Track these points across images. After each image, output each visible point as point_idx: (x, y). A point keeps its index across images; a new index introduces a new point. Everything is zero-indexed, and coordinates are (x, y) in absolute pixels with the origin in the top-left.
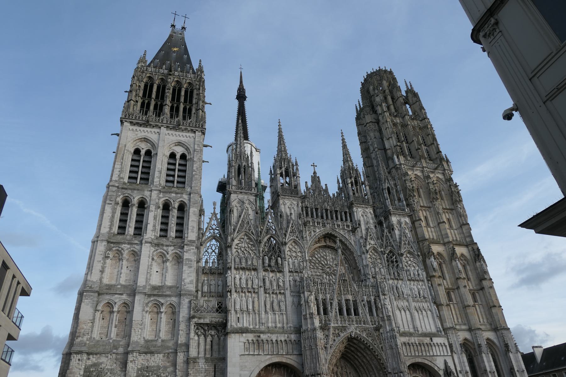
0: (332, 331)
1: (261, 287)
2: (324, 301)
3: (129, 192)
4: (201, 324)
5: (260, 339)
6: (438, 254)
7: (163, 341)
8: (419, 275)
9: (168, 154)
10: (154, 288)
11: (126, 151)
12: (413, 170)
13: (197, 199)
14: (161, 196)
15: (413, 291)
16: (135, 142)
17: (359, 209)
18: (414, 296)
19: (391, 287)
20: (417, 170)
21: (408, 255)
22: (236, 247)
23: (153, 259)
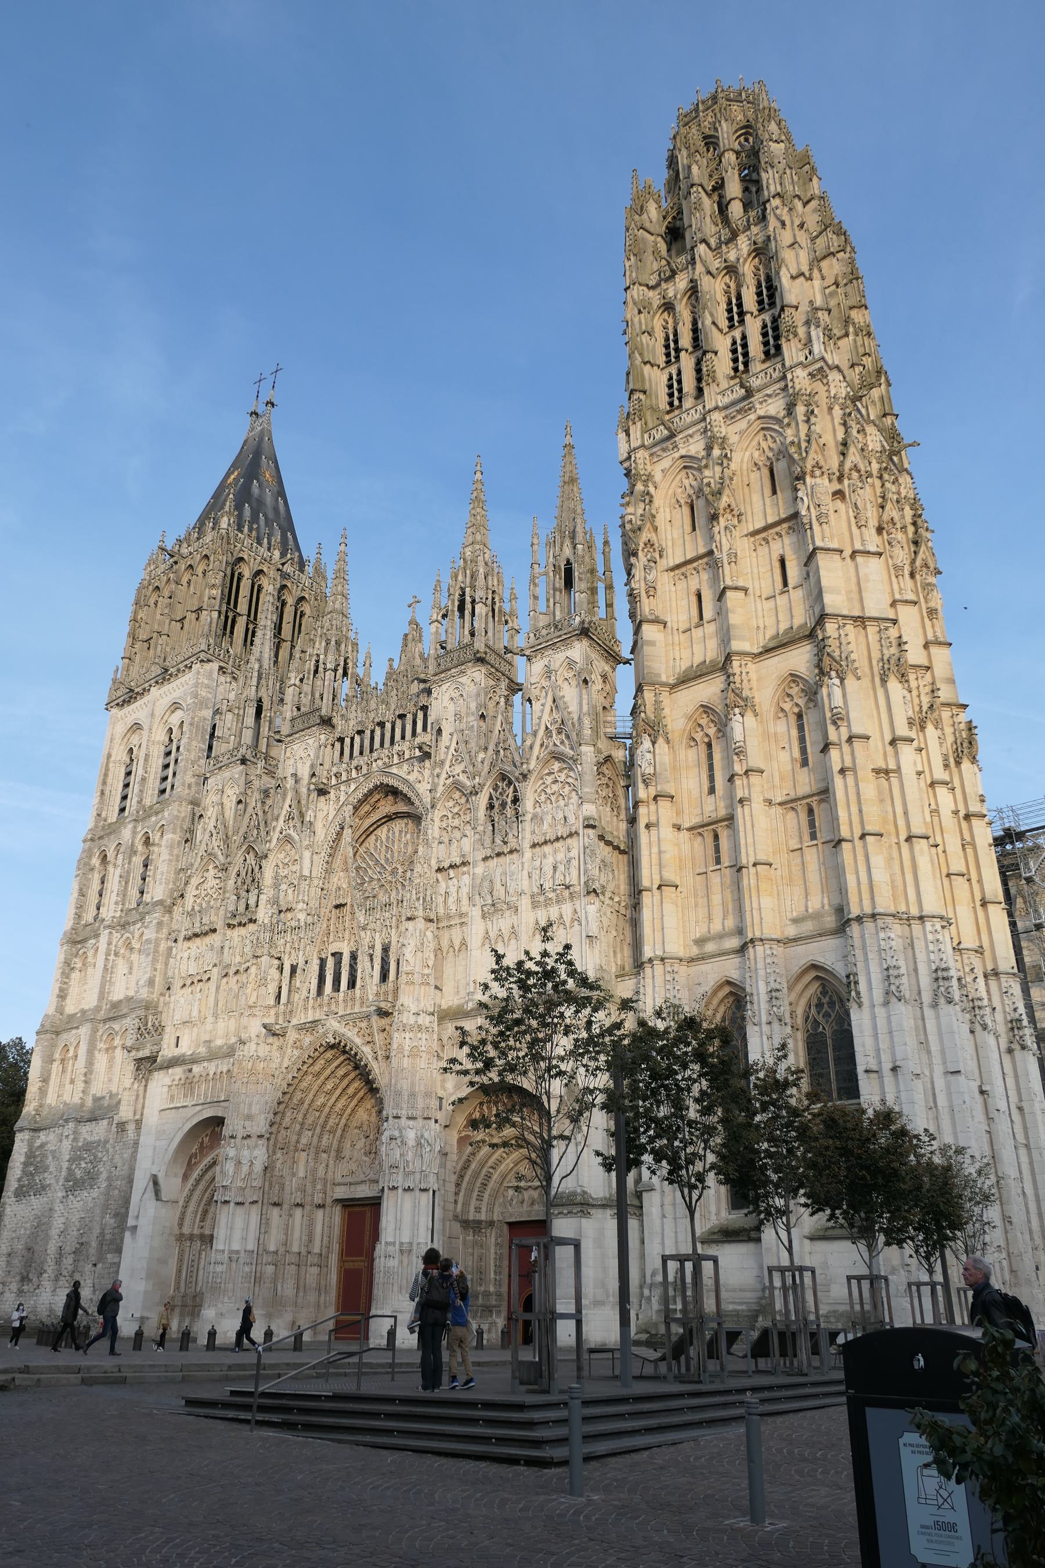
0: (292, 1035)
1: (215, 965)
2: (294, 969)
3: (105, 841)
4: (141, 1059)
5: (191, 1075)
6: (705, 712)
7: (111, 1096)
8: (565, 818)
9: (161, 736)
10: (115, 1005)
11: (111, 765)
12: (676, 446)
13: (176, 813)
14: (139, 829)
15: (536, 875)
16: (125, 740)
17: (444, 687)
18: (536, 890)
19: (478, 881)
20: (691, 436)
21: (557, 766)
22: (198, 892)
23: (116, 954)
